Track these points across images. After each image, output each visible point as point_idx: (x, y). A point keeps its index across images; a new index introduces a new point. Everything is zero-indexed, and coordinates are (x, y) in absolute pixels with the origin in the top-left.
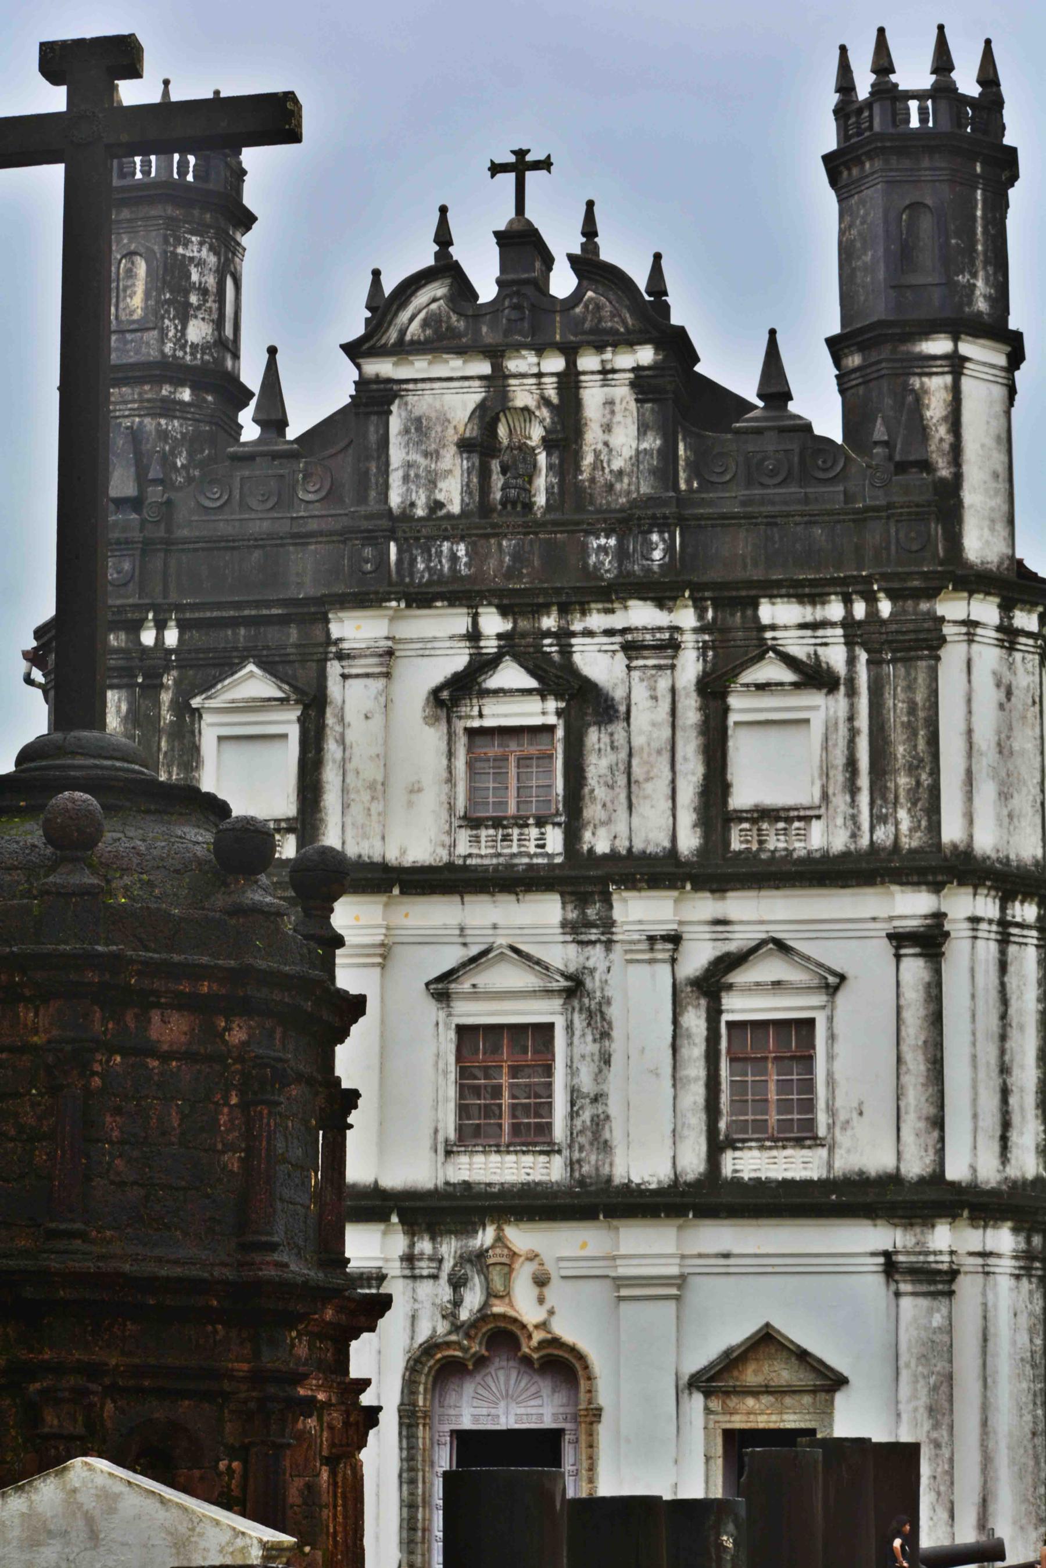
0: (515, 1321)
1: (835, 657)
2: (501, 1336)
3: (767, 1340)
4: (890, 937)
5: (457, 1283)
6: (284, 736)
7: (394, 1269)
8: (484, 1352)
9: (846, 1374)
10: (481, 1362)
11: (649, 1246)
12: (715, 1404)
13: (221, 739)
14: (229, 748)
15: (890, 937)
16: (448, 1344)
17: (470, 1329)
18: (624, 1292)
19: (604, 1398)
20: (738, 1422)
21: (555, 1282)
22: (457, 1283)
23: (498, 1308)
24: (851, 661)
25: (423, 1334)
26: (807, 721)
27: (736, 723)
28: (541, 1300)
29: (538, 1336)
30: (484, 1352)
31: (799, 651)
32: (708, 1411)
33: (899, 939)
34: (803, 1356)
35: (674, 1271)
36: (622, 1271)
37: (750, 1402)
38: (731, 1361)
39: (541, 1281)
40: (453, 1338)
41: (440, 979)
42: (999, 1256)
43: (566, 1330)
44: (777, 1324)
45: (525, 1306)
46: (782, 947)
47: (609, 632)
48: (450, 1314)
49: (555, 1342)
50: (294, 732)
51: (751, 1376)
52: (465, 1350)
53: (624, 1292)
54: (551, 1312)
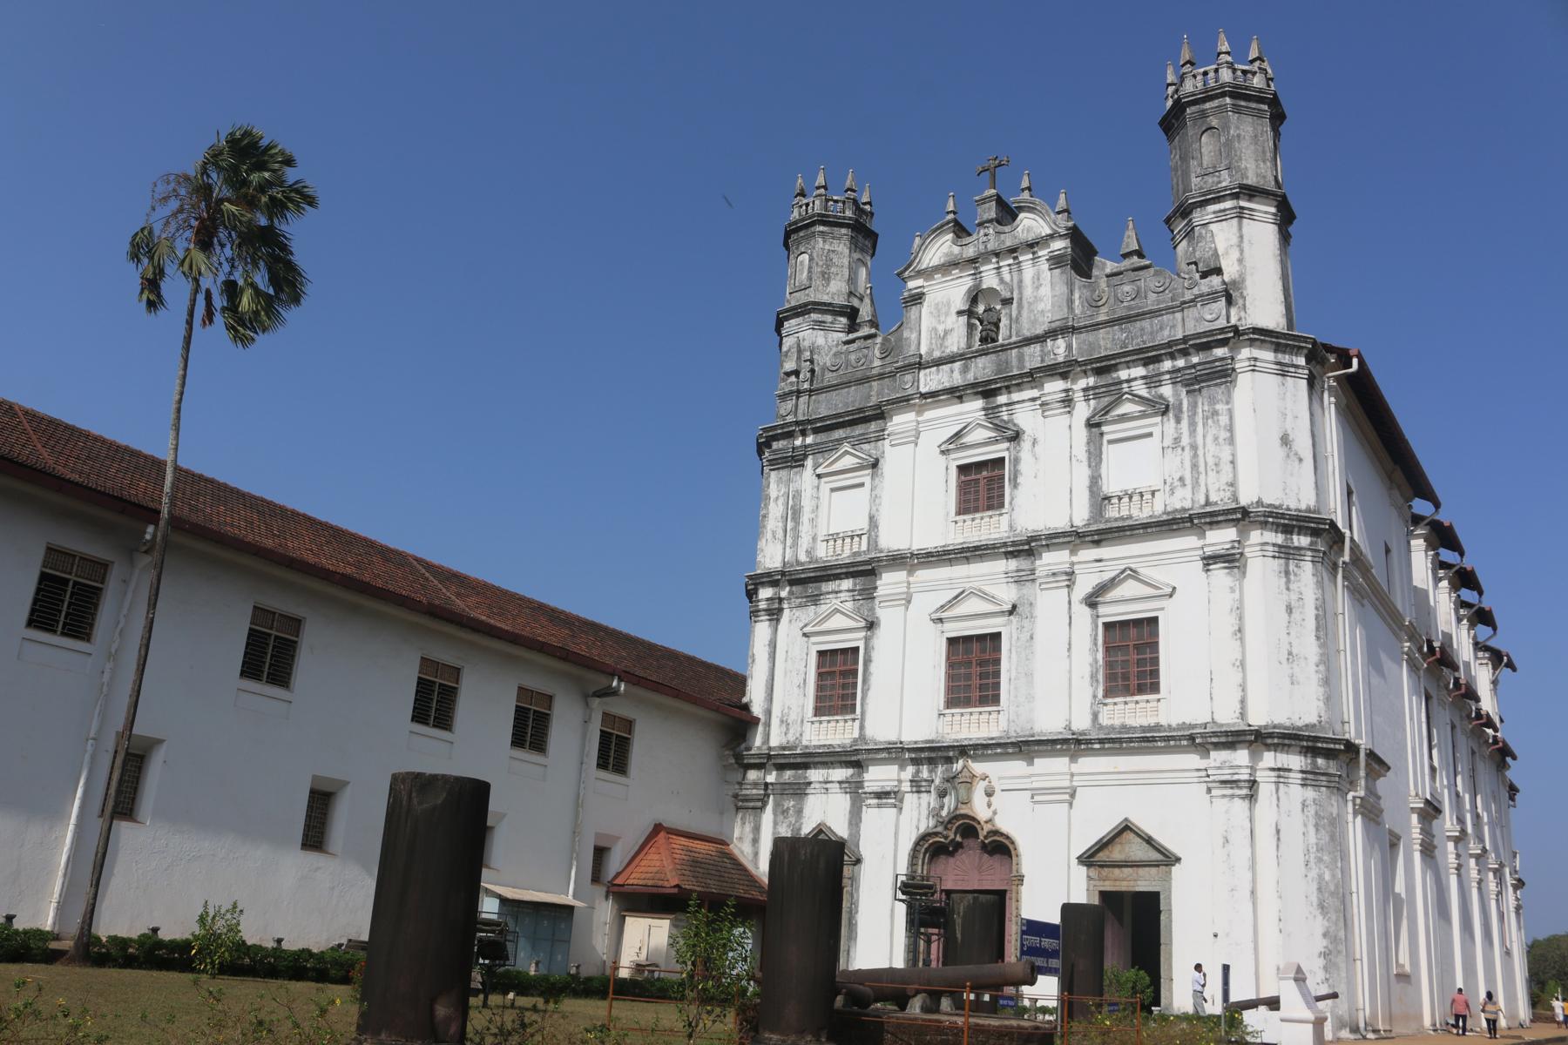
0: (974, 819)
1: (1167, 391)
2: (969, 828)
3: (1126, 828)
4: (1204, 559)
5: (942, 794)
6: (862, 485)
7: (906, 787)
8: (958, 839)
9: (1179, 855)
10: (958, 846)
11: (1053, 768)
12: (1094, 872)
13: (833, 490)
14: (835, 494)
15: (1204, 559)
16: (936, 834)
17: (947, 824)
18: (1037, 798)
19: (1025, 870)
20: (1108, 887)
21: (998, 793)
22: (942, 794)
23: (964, 810)
24: (1176, 394)
25: (922, 830)
26: (1150, 435)
27: (1110, 442)
28: (989, 805)
29: (987, 828)
30: (958, 839)
31: (1144, 392)
32: (1089, 878)
33: (1209, 560)
34: (1149, 841)
35: (1067, 783)
36: (1035, 785)
37: (1117, 871)
38: (1103, 845)
39: (989, 793)
40: (939, 829)
41: (937, 611)
42: (1289, 770)
43: (1003, 824)
44: (1132, 819)
45: (980, 808)
46: (1133, 574)
47: (1033, 400)
48: (935, 813)
49: (996, 832)
50: (867, 480)
51: (1116, 853)
52: (946, 837)
53: (1037, 798)
54: (995, 813)
